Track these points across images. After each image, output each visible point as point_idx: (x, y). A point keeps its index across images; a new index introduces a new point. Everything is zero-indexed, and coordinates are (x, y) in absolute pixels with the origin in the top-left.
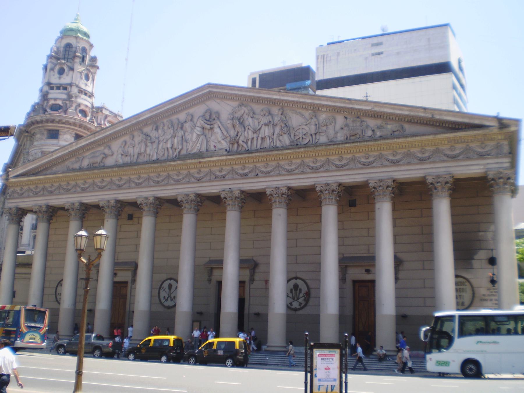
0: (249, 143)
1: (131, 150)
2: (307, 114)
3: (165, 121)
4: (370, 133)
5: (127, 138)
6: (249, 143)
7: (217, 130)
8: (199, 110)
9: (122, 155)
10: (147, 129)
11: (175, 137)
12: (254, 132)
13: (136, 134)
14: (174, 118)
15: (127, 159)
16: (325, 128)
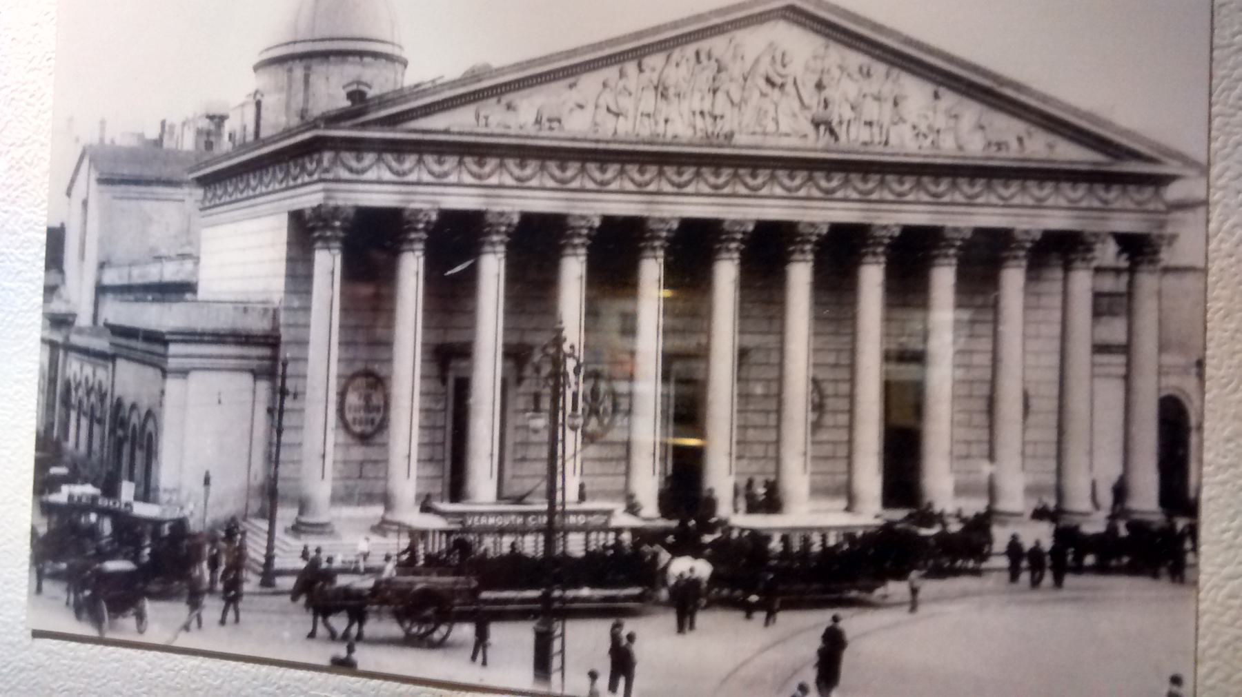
0: (844, 126)
1: (626, 103)
2: (929, 88)
3: (690, 50)
4: (1014, 144)
5: (611, 73)
6: (844, 126)
7: (790, 88)
8: (754, 41)
9: (608, 110)
10: (655, 61)
11: (715, 92)
12: (853, 108)
13: (631, 67)
14: (704, 45)
15: (624, 127)
16: (952, 122)
